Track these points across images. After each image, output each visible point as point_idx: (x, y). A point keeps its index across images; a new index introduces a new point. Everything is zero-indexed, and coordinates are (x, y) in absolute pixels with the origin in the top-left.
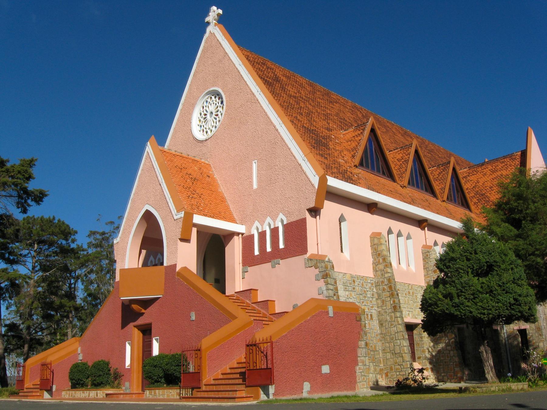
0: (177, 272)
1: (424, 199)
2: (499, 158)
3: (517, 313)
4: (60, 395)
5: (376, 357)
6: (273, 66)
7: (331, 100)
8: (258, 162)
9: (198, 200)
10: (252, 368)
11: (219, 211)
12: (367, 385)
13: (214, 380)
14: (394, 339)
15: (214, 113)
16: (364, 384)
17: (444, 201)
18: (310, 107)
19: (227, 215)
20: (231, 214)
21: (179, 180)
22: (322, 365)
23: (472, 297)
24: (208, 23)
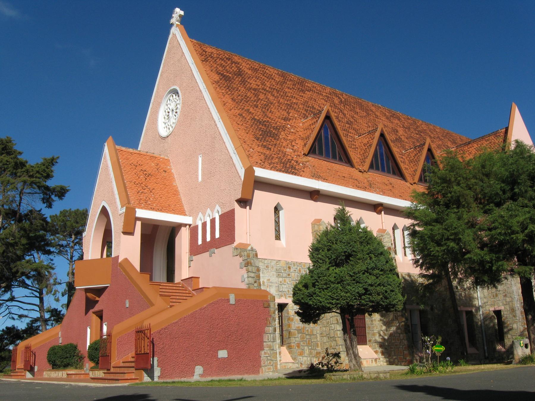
0: (120, 263)
1: (387, 182)
2: (485, 136)
3: (368, 303)
4: (42, 375)
5: (312, 341)
6: (239, 61)
7: (303, 89)
8: (202, 156)
9: (148, 195)
10: (139, 353)
11: (168, 204)
12: (273, 369)
13: (123, 362)
14: (330, 323)
15: (175, 111)
16: (270, 368)
17: (414, 183)
18: (271, 98)
19: (177, 207)
20: (181, 205)
21: (132, 176)
22: (218, 350)
23: (325, 287)
24: (172, 24)
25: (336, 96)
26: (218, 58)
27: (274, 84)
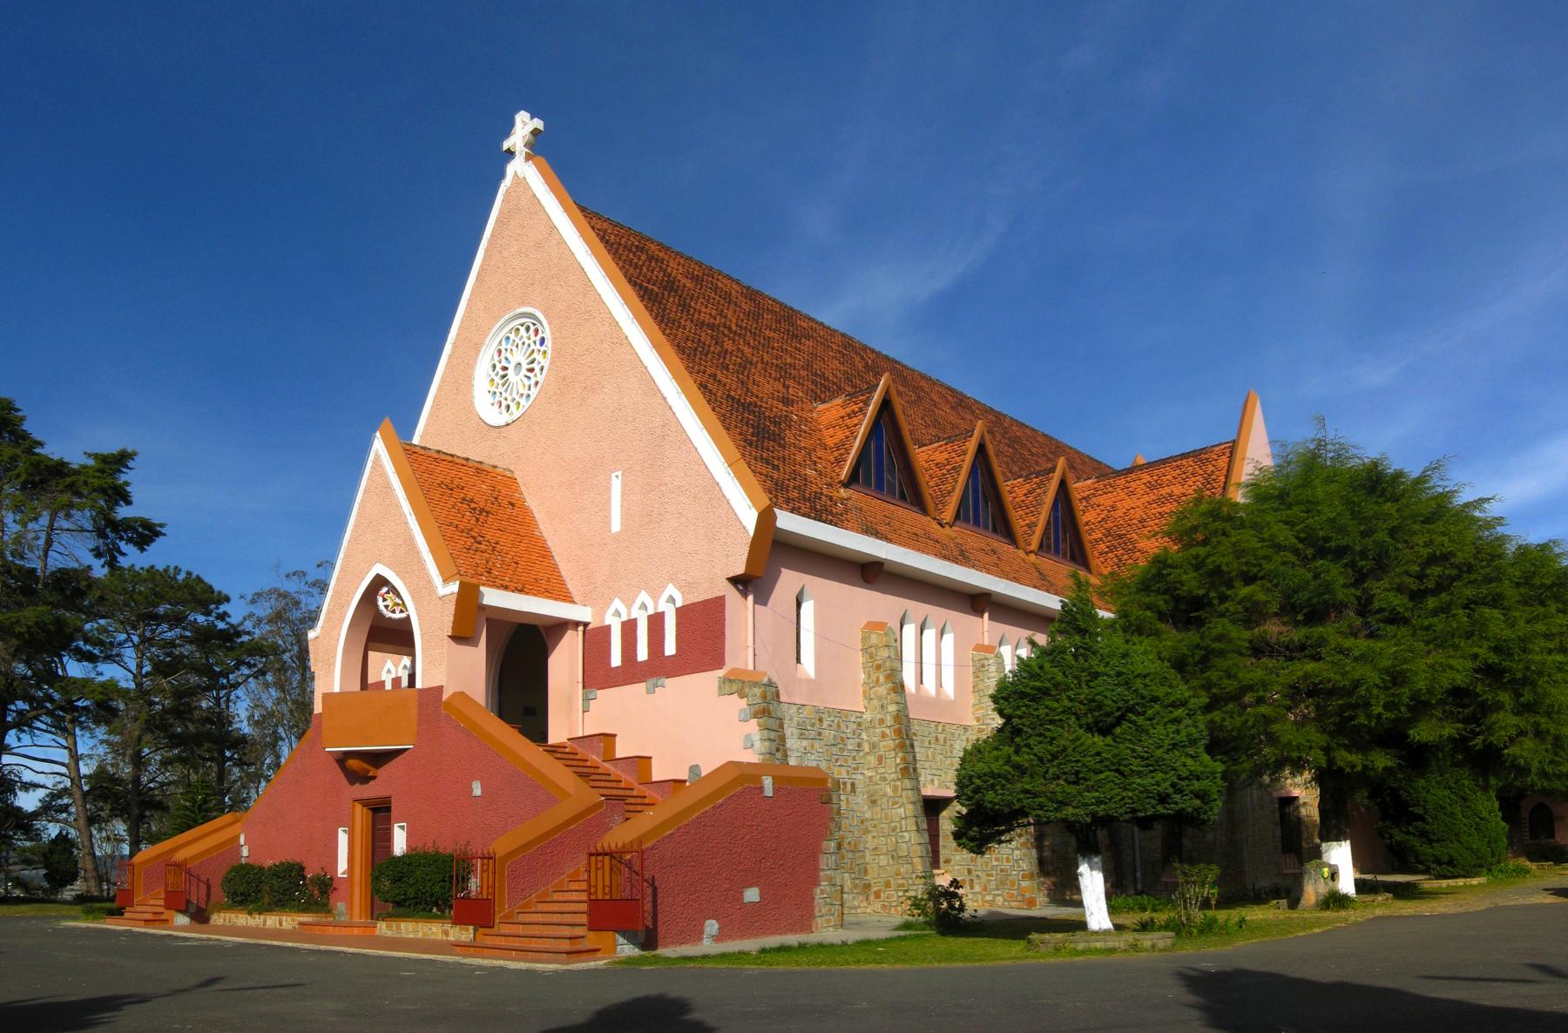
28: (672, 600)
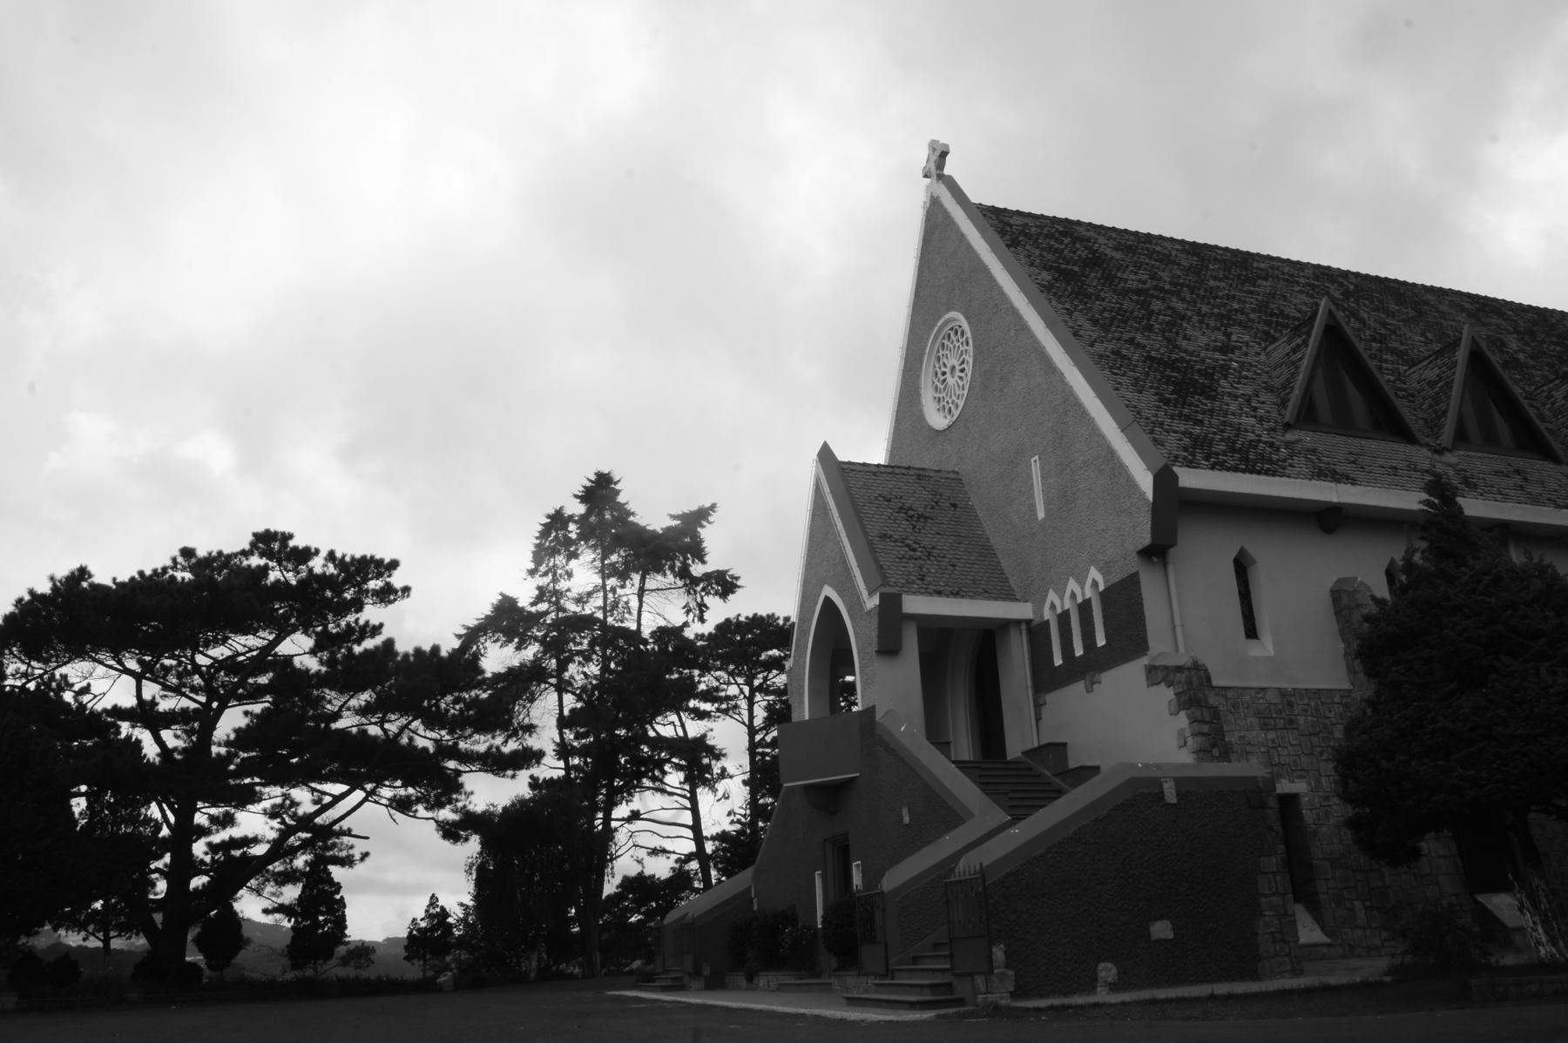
8: (1040, 459)
15: (958, 368)
18: (1180, 306)
19: (994, 584)
25: (1333, 282)
26: (1040, 234)
27: (1179, 273)
28: (1095, 584)
